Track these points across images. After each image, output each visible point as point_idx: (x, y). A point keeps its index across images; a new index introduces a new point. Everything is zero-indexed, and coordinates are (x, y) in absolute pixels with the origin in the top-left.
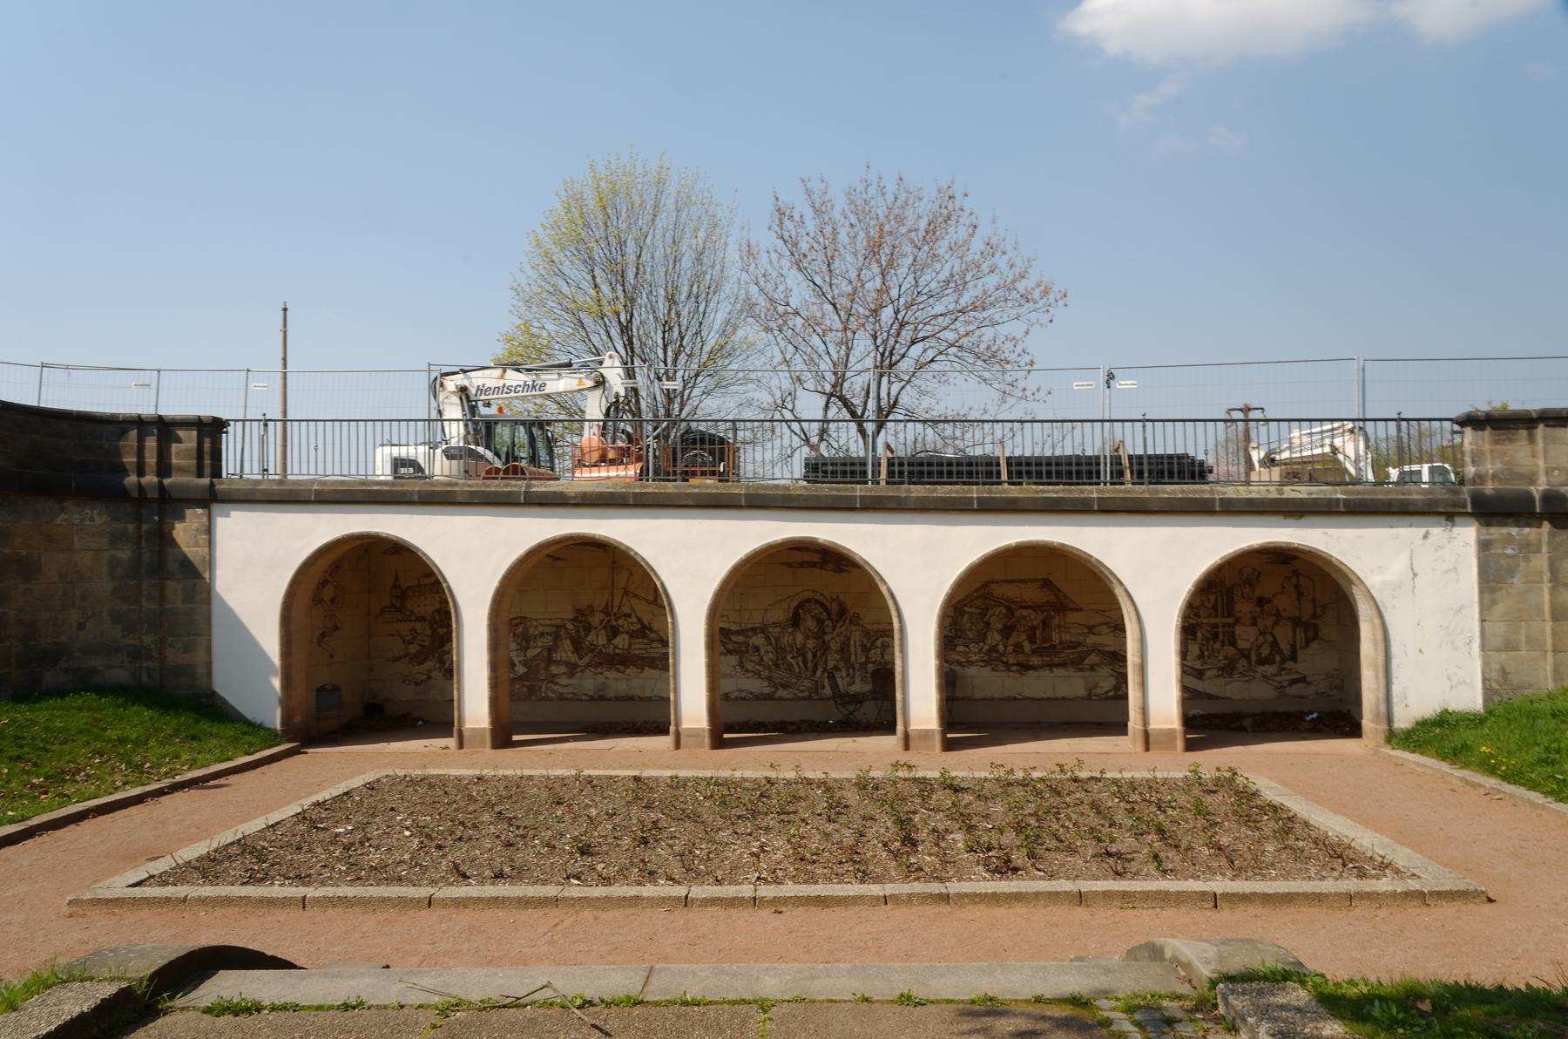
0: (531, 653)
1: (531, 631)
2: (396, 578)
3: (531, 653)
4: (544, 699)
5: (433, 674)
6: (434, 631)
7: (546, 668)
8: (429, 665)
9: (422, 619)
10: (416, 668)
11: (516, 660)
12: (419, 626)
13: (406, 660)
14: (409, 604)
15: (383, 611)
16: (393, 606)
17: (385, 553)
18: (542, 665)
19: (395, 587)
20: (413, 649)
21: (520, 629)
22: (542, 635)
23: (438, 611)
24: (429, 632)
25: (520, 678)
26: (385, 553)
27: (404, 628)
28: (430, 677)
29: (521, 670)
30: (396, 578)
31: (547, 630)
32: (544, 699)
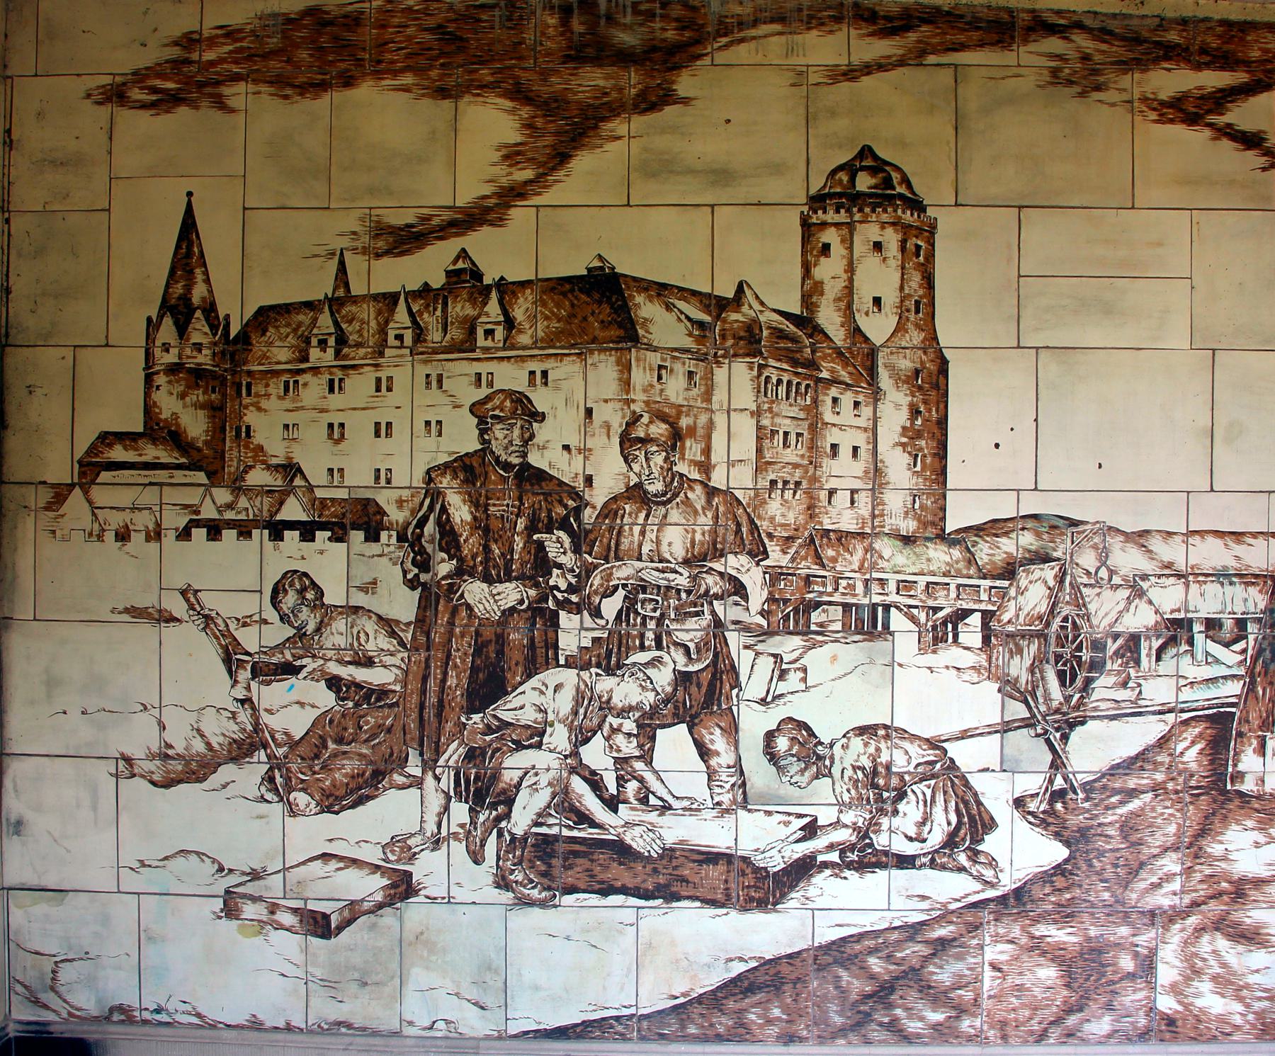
0: (1092, 750)
1: (1105, 609)
2: (188, 253)
3: (1092, 750)
4: (1170, 1028)
5: (428, 869)
6: (432, 598)
7: (1193, 847)
8: (395, 811)
9: (362, 518)
10: (313, 830)
11: (995, 795)
12: (329, 563)
13: (250, 775)
14: (266, 424)
15: (91, 468)
16: (158, 429)
17: (115, 95)
18: (1168, 824)
19: (178, 309)
20: (295, 707)
21: (1032, 594)
22: (1176, 631)
23: (468, 469)
24: (404, 605)
25: (1016, 901)
26: (115, 95)
27: (233, 573)
28: (403, 888)
29: (1022, 851)
30: (188, 253)
31: (1209, 601)
32: (1170, 1028)
